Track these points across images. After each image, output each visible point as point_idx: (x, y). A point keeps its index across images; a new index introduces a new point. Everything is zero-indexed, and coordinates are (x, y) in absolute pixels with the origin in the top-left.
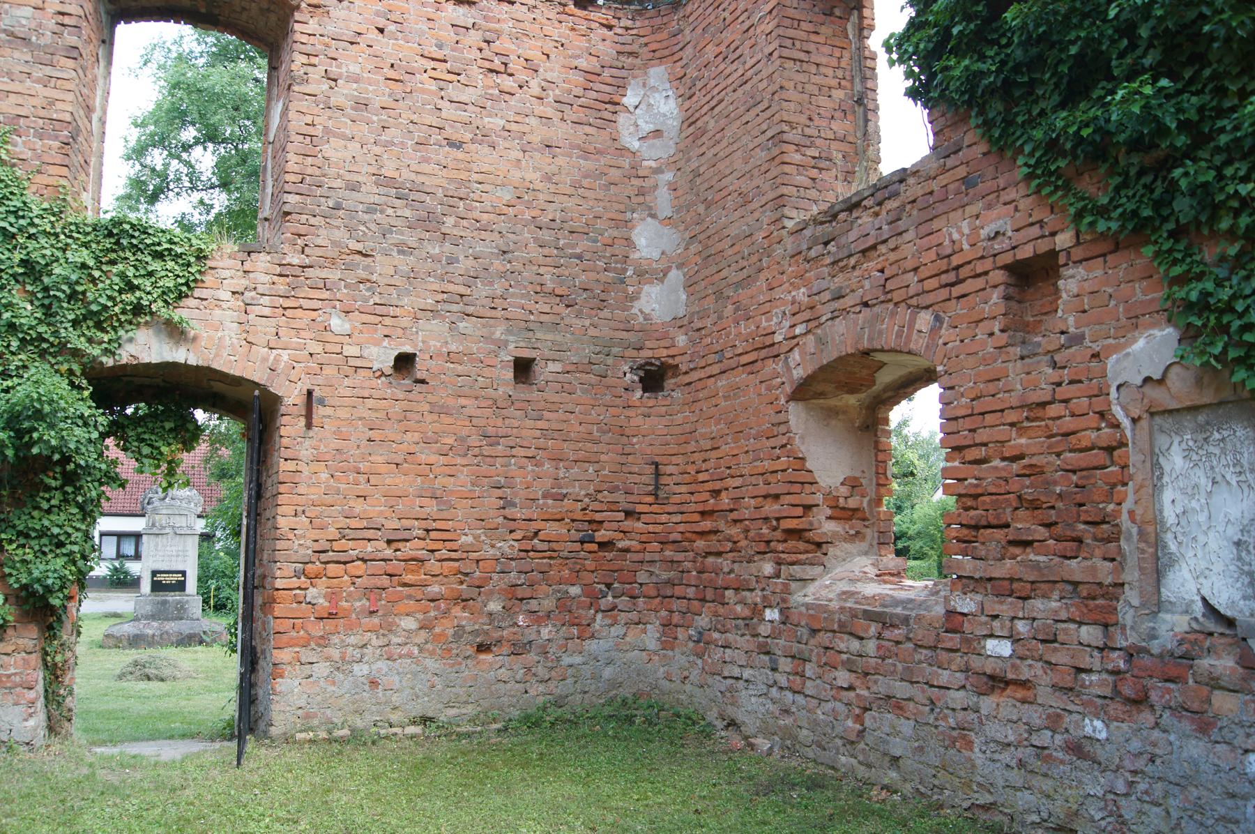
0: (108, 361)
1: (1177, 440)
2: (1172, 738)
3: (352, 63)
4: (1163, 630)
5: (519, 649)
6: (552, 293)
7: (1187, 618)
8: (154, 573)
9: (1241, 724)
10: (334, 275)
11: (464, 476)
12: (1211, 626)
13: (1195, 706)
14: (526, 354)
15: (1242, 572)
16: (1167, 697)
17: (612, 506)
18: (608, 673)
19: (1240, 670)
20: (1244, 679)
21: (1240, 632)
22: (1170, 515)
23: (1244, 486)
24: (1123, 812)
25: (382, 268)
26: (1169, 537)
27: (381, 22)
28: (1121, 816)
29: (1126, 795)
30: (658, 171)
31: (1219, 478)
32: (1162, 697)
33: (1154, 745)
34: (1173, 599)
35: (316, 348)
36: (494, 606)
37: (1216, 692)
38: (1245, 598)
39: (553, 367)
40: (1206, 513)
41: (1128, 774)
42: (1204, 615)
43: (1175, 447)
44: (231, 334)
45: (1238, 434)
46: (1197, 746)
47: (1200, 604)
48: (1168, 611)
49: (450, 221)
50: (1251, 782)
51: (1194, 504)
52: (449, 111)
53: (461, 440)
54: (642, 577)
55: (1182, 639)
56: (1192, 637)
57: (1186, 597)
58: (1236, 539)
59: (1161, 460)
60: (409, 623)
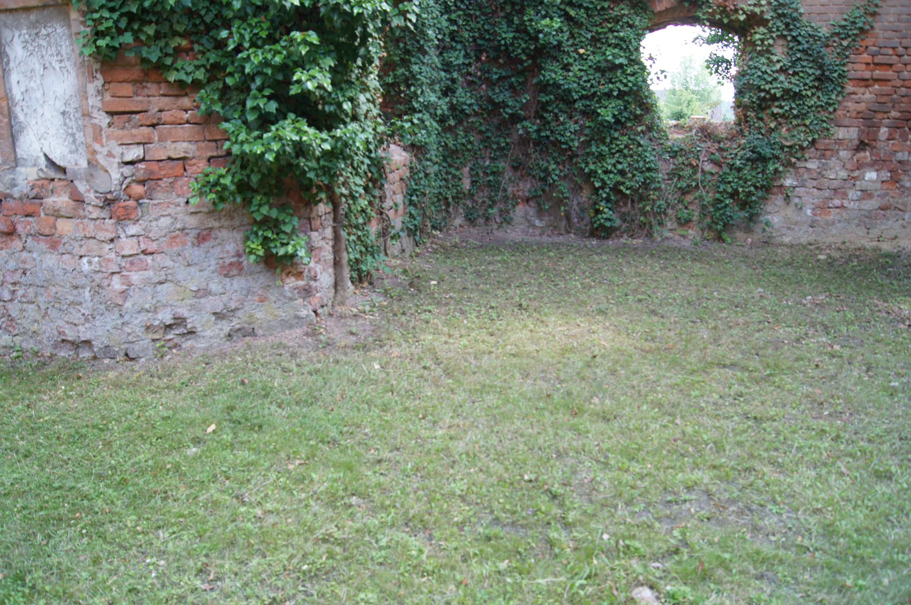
1: (17, 34)
2: (35, 255)
4: (20, 180)
7: (35, 169)
9: (75, 239)
12: (52, 174)
13: (47, 232)
15: (68, 134)
16: (28, 227)
19: (72, 203)
20: (75, 209)
21: (69, 176)
22: (17, 92)
23: (64, 71)
24: (11, 313)
26: (17, 110)
28: (9, 316)
29: (11, 300)
31: (47, 65)
32: (25, 228)
33: (24, 262)
34: (25, 157)
37: (59, 220)
38: (71, 152)
40: (41, 91)
41: (10, 286)
42: (46, 167)
43: (16, 39)
45: (58, 31)
46: (51, 259)
47: (43, 158)
48: (23, 165)
50: (86, 277)
51: (32, 84)
55: (34, 185)
56: (40, 183)
57: (34, 154)
58: (62, 110)
59: (7, 49)
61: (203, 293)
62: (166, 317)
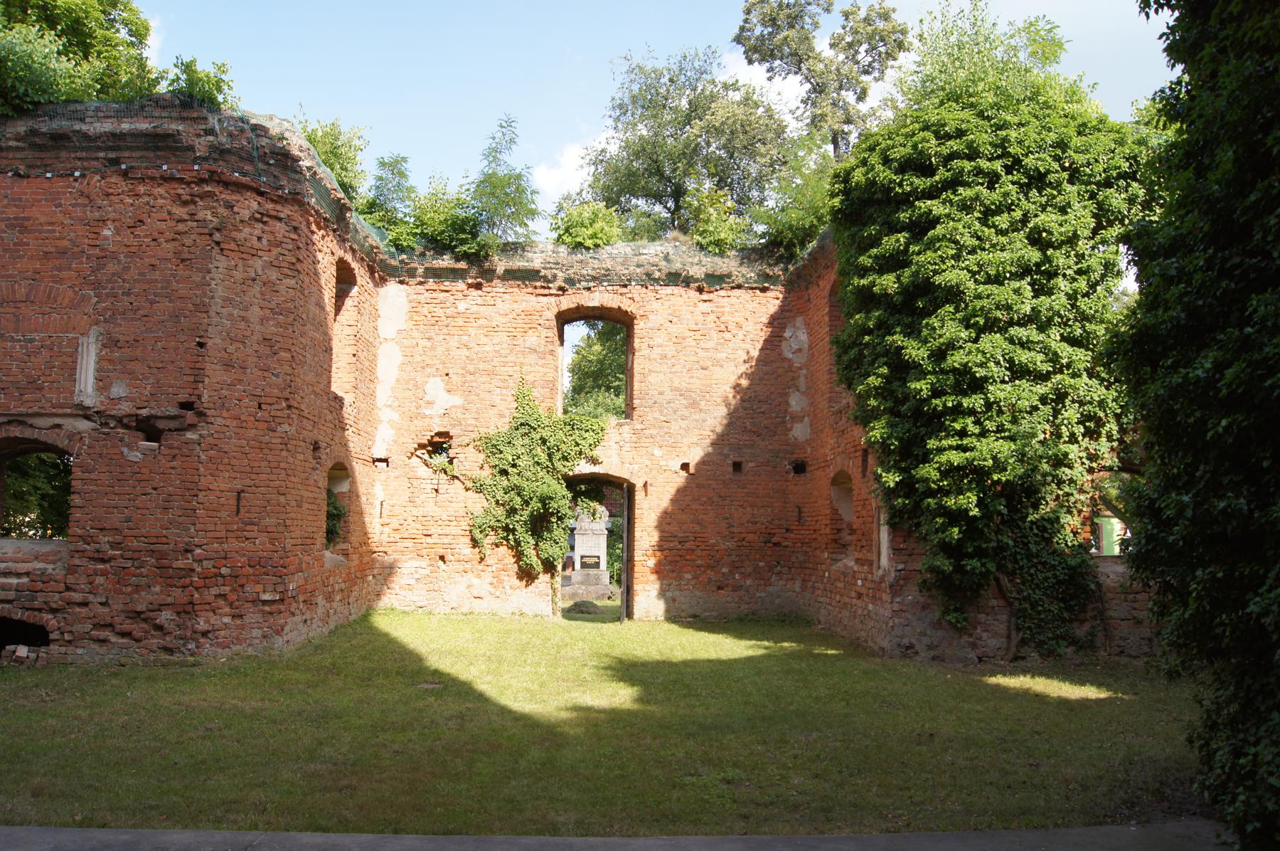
0: (571, 473)
3: (660, 338)
5: (736, 588)
6: (750, 431)
8: (582, 557)
10: (654, 432)
11: (711, 515)
14: (738, 459)
17: (780, 526)
18: (777, 601)
25: (674, 426)
27: (671, 318)
30: (800, 368)
35: (649, 463)
36: (725, 570)
39: (751, 465)
44: (616, 460)
49: (703, 403)
52: (701, 353)
53: (710, 499)
54: (793, 559)
60: (688, 576)
61: (923, 634)
62: (906, 641)
